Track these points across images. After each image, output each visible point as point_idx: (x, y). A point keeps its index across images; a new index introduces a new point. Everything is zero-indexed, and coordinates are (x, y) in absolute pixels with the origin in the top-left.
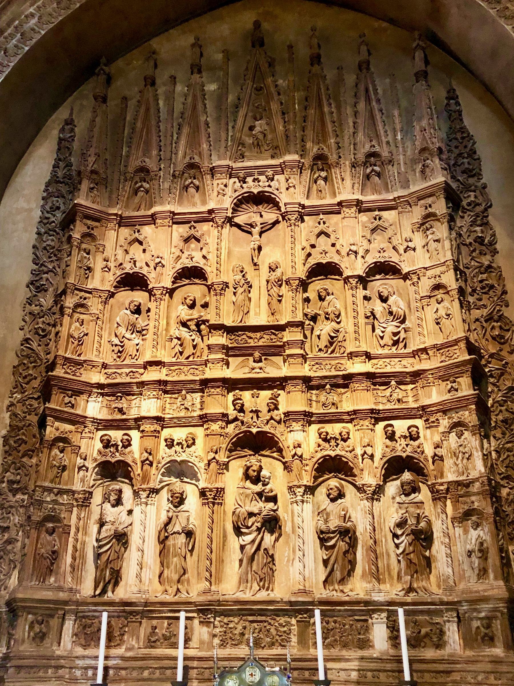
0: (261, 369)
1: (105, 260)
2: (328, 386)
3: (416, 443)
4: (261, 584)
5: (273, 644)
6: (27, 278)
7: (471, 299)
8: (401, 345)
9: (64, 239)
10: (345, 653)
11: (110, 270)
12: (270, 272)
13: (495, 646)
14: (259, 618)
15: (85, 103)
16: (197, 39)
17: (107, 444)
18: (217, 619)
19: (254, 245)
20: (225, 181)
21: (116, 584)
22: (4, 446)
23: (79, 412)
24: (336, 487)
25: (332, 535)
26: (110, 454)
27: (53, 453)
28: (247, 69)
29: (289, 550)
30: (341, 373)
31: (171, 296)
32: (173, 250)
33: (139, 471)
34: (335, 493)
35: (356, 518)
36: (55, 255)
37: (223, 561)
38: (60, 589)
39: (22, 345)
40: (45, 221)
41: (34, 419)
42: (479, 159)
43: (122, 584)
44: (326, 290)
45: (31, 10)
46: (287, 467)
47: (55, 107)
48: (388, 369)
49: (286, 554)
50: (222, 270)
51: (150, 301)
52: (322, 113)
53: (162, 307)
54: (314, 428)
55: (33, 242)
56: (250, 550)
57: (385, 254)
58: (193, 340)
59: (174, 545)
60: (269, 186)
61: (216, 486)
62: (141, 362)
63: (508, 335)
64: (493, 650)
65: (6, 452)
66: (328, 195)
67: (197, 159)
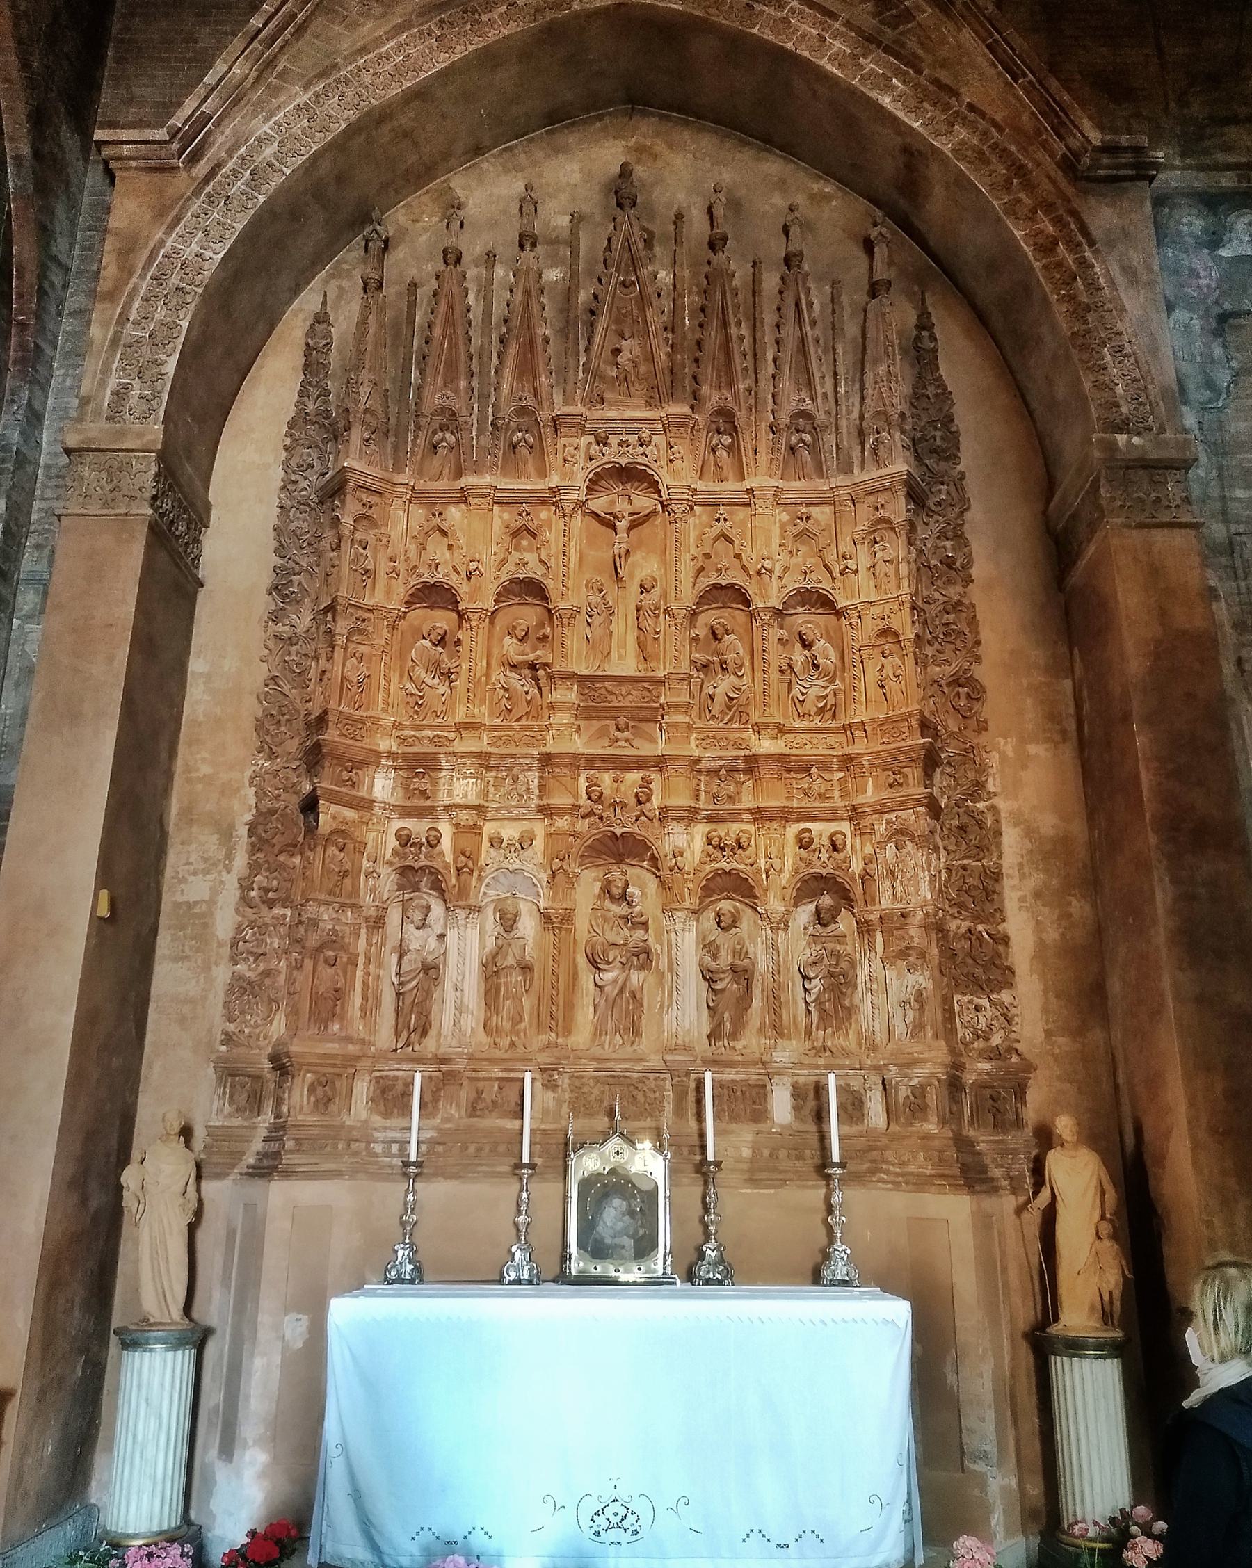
0: (627, 740)
1: (391, 559)
2: (723, 772)
3: (841, 856)
6: (267, 579)
7: (929, 651)
8: (828, 715)
11: (398, 575)
12: (642, 592)
15: (345, 283)
16: (528, 188)
17: (405, 840)
19: (620, 548)
20: (575, 441)
21: (424, 1033)
22: (250, 837)
23: (363, 793)
24: (730, 912)
25: (722, 976)
26: (411, 856)
27: (329, 852)
28: (609, 248)
29: (664, 993)
30: (742, 753)
31: (492, 622)
32: (494, 548)
33: (454, 881)
34: (727, 920)
35: (755, 954)
38: (348, 1039)
42: (957, 432)
43: (432, 1033)
44: (724, 625)
45: (266, 128)
46: (663, 884)
48: (808, 751)
49: (659, 999)
50: (570, 586)
51: (460, 627)
52: (728, 338)
53: (480, 639)
54: (700, 830)
55: (274, 521)
56: (612, 991)
57: (814, 577)
58: (527, 693)
59: (506, 984)
60: (644, 454)
61: (565, 906)
62: (450, 721)
63: (976, 706)
65: (253, 845)
66: (731, 475)
67: (530, 401)
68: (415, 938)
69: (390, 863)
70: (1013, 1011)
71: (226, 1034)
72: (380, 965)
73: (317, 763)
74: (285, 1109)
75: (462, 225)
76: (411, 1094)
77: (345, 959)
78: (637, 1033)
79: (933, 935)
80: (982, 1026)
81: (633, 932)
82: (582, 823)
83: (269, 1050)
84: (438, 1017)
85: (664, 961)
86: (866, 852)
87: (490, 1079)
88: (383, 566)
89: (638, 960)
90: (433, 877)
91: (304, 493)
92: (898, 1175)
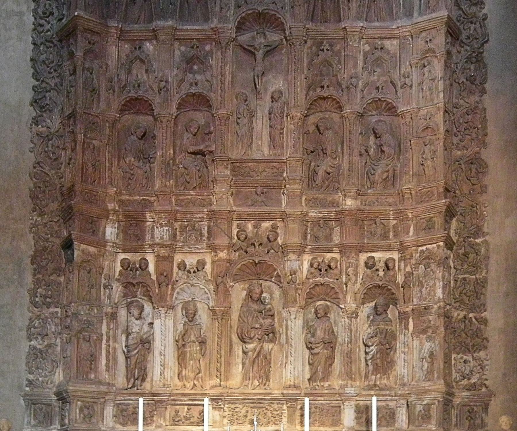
3: (391, 273)
4: (260, 381)
5: (269, 423)
6: (29, 96)
9: (65, 54)
12: (272, 102)
13: (431, 424)
14: (258, 405)
18: (226, 405)
21: (143, 380)
35: (338, 332)
36: (55, 71)
37: (230, 364)
38: (100, 383)
39: (35, 168)
41: (58, 242)
43: (148, 379)
65: (35, 269)
68: (136, 326)
69: (118, 280)
70: (486, 363)
72: (115, 341)
73: (70, 218)
74: (67, 421)
76: (137, 414)
77: (95, 338)
78: (268, 379)
79: (442, 319)
80: (467, 372)
81: (265, 320)
82: (235, 255)
83: (55, 389)
84: (151, 371)
85: (284, 336)
86: (407, 270)
87: (183, 405)
88: (104, 85)
89: (268, 337)
90: (145, 288)
91: (49, 33)
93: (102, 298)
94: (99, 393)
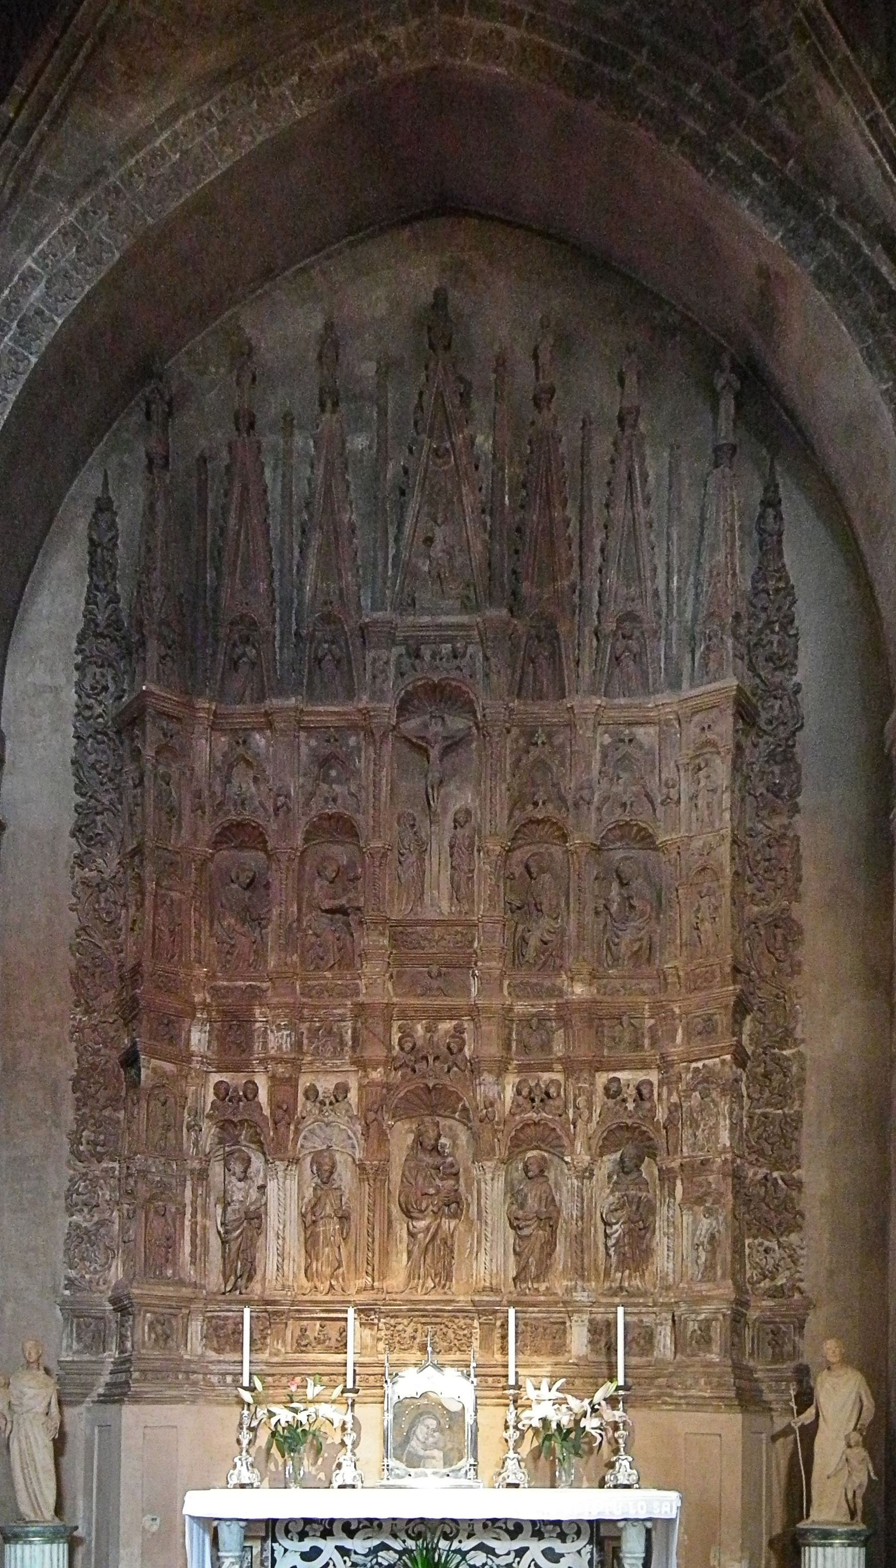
0: (439, 988)
3: (647, 1105)
4: (437, 1280)
5: (451, 1349)
6: (69, 820)
7: (749, 888)
10: (536, 1359)
12: (455, 827)
13: (710, 1352)
14: (434, 1320)
20: (384, 654)
21: (250, 1278)
35: (560, 1201)
36: (110, 780)
38: (181, 1283)
40: (87, 713)
41: (115, 1055)
43: (258, 1277)
47: (75, 468)
55: (70, 754)
64: (708, 1355)
65: (78, 1100)
69: (209, 1116)
71: (68, 1279)
72: (205, 1215)
73: (134, 1017)
74: (129, 1345)
75: (254, 379)
76: (241, 1333)
77: (173, 1210)
78: (449, 1278)
79: (729, 1180)
80: (770, 1267)
85: (474, 1208)
87: (313, 1319)
89: (449, 1210)
90: (252, 1131)
91: (100, 720)
92: (680, 1398)
93: (185, 1146)
94: (181, 1299)
